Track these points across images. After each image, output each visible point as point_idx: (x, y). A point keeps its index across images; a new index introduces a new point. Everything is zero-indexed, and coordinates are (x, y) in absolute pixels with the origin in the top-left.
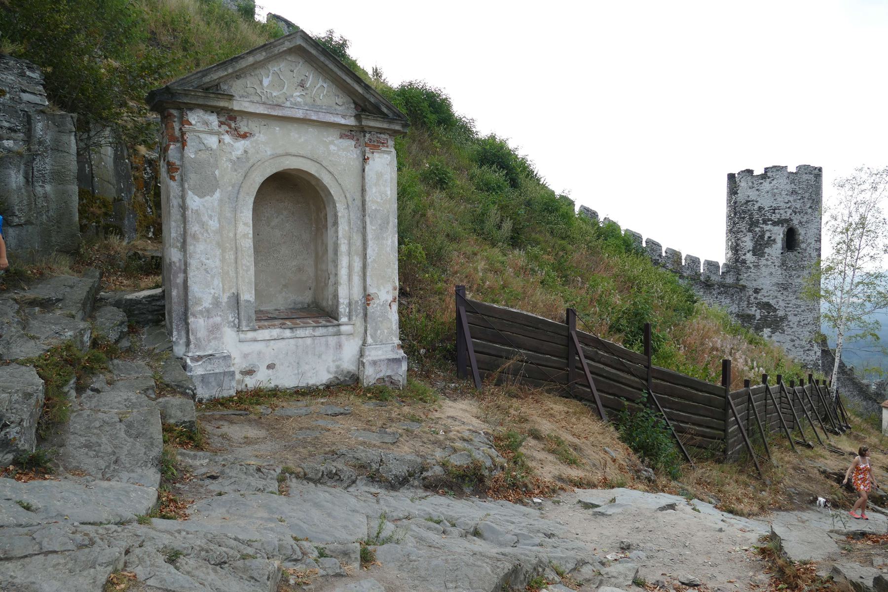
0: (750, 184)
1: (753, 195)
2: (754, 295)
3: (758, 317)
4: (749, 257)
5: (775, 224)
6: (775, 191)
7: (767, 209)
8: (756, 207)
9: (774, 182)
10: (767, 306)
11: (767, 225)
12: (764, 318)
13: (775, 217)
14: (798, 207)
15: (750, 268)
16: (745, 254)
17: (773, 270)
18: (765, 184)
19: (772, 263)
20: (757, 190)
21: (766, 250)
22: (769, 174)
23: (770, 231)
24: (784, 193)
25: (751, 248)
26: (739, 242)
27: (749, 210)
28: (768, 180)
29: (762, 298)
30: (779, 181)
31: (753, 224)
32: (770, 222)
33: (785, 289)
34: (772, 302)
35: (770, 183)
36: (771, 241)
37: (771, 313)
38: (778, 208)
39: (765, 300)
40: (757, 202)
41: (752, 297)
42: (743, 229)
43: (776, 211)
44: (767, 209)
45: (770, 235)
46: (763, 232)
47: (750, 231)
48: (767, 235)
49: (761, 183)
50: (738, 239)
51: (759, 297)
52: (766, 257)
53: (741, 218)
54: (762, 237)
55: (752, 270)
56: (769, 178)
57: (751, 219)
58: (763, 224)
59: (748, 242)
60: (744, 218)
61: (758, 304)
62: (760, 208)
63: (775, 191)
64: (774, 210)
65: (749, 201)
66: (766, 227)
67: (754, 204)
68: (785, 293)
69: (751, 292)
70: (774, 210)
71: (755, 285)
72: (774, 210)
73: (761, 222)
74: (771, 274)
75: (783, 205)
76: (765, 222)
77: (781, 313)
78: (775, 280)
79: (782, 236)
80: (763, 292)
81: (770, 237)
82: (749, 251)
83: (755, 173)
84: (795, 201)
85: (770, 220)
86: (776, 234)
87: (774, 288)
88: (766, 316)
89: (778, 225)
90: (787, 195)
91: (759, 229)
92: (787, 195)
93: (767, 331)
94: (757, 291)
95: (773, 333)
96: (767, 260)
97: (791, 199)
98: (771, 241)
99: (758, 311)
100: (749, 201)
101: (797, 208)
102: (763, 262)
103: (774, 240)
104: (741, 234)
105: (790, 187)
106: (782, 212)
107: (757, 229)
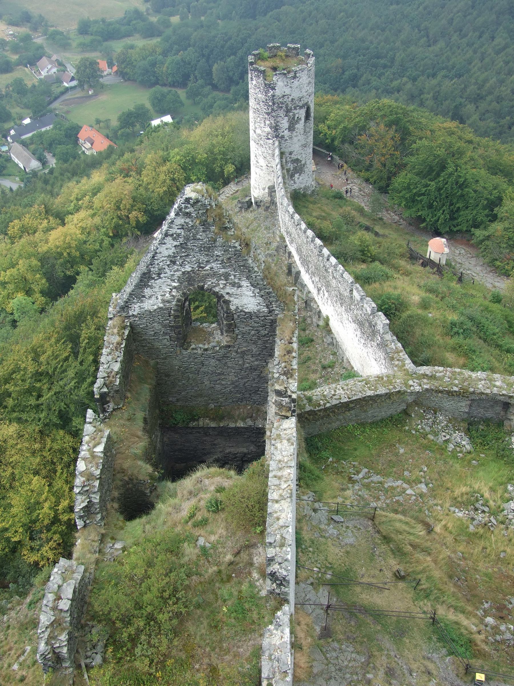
0: (286, 83)
1: (287, 91)
3: (292, 168)
4: (286, 133)
7: (296, 99)
8: (290, 99)
10: (297, 161)
11: (296, 109)
12: (295, 168)
13: (301, 104)
15: (287, 140)
16: (283, 132)
18: (295, 82)
21: (297, 126)
22: (297, 75)
24: (305, 85)
26: (278, 124)
31: (288, 111)
33: (305, 147)
34: (299, 157)
36: (299, 119)
38: (302, 97)
39: (296, 157)
42: (282, 115)
44: (296, 99)
46: (294, 115)
47: (286, 116)
48: (297, 116)
54: (294, 118)
57: (287, 107)
59: (285, 123)
60: (282, 107)
62: (292, 99)
69: (287, 155)
70: (300, 99)
71: (290, 150)
75: (305, 94)
77: (303, 162)
80: (295, 153)
85: (298, 106)
87: (301, 148)
88: (296, 167)
94: (291, 153)
95: (300, 175)
97: (308, 88)
98: (299, 119)
106: (304, 99)
107: (291, 114)
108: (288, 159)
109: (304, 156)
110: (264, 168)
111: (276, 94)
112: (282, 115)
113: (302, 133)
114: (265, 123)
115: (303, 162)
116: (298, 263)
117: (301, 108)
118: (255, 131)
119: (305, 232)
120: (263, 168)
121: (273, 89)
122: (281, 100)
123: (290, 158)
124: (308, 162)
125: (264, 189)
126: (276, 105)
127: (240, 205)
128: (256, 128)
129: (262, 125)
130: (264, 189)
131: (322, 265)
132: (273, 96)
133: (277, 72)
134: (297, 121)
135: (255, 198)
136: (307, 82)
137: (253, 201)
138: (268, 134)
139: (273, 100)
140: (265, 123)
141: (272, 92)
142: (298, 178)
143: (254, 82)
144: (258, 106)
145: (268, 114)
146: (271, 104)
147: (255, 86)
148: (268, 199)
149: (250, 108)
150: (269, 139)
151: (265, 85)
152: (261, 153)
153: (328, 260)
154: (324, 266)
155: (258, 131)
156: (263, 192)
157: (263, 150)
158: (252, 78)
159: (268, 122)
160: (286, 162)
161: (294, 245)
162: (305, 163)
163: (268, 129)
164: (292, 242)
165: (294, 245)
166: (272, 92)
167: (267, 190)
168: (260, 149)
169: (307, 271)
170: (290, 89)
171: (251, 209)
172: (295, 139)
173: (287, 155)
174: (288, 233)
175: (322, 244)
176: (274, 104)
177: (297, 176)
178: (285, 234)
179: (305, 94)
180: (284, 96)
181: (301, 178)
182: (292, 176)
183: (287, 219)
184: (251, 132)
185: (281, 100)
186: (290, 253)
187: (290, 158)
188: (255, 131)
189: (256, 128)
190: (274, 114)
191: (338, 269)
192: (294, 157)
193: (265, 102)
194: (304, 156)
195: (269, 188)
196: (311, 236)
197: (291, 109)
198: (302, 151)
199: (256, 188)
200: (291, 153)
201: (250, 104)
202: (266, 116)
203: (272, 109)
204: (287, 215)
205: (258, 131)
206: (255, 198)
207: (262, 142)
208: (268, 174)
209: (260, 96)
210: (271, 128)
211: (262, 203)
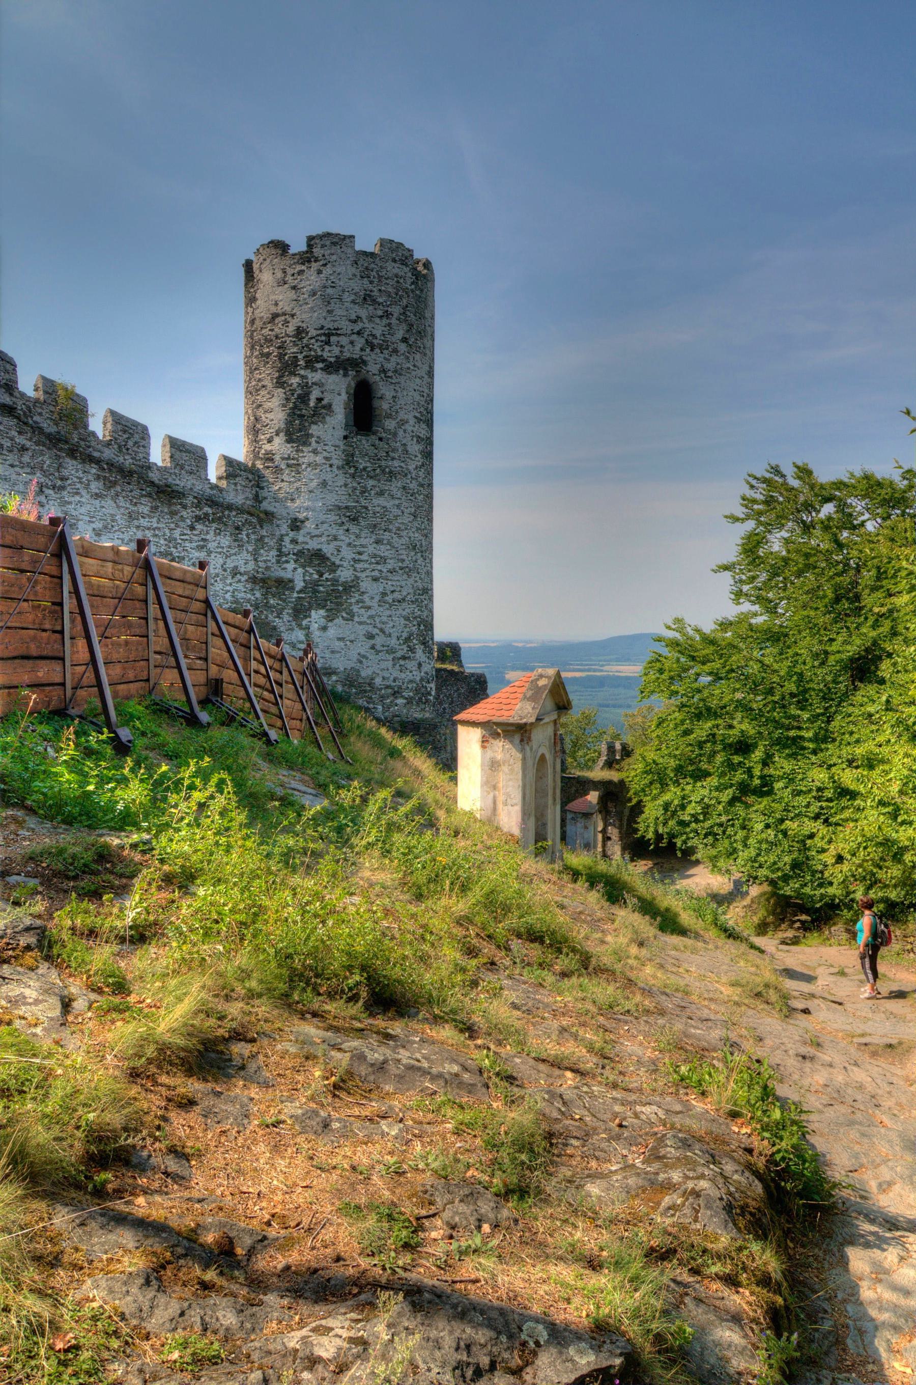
0: (279, 275)
2: (292, 534)
3: (299, 585)
5: (331, 368)
7: (313, 333)
8: (291, 329)
9: (328, 270)
11: (314, 370)
12: (312, 587)
13: (330, 353)
14: (378, 333)
19: (326, 458)
20: (294, 288)
21: (314, 430)
22: (317, 251)
24: (347, 297)
26: (260, 412)
27: (277, 337)
28: (315, 266)
29: (307, 539)
30: (339, 270)
32: (320, 365)
33: (354, 520)
35: (319, 272)
37: (326, 576)
38: (336, 332)
39: (313, 545)
40: (293, 316)
41: (287, 539)
43: (333, 339)
45: (320, 395)
48: (315, 394)
49: (301, 272)
51: (301, 539)
52: (314, 444)
54: (304, 398)
57: (281, 356)
60: (268, 355)
61: (299, 554)
64: (328, 335)
66: (314, 377)
67: (286, 322)
68: (354, 529)
69: (284, 528)
70: (328, 335)
72: (328, 335)
73: (302, 363)
76: (310, 363)
77: (345, 574)
79: (344, 396)
80: (309, 526)
81: (320, 400)
83: (292, 251)
84: (371, 318)
86: (332, 391)
87: (332, 517)
88: (316, 583)
89: (337, 371)
90: (353, 302)
92: (353, 302)
93: (317, 616)
95: (329, 618)
96: (315, 452)
97: (363, 313)
99: (300, 570)
101: (374, 336)
103: (329, 407)
104: (263, 392)
105: (358, 285)
106: (344, 340)
107: (295, 381)
108: (288, 546)
112: (267, 382)
113: (335, 462)
123: (294, 541)
142: (324, 629)
170: (292, 295)
180: (275, 316)
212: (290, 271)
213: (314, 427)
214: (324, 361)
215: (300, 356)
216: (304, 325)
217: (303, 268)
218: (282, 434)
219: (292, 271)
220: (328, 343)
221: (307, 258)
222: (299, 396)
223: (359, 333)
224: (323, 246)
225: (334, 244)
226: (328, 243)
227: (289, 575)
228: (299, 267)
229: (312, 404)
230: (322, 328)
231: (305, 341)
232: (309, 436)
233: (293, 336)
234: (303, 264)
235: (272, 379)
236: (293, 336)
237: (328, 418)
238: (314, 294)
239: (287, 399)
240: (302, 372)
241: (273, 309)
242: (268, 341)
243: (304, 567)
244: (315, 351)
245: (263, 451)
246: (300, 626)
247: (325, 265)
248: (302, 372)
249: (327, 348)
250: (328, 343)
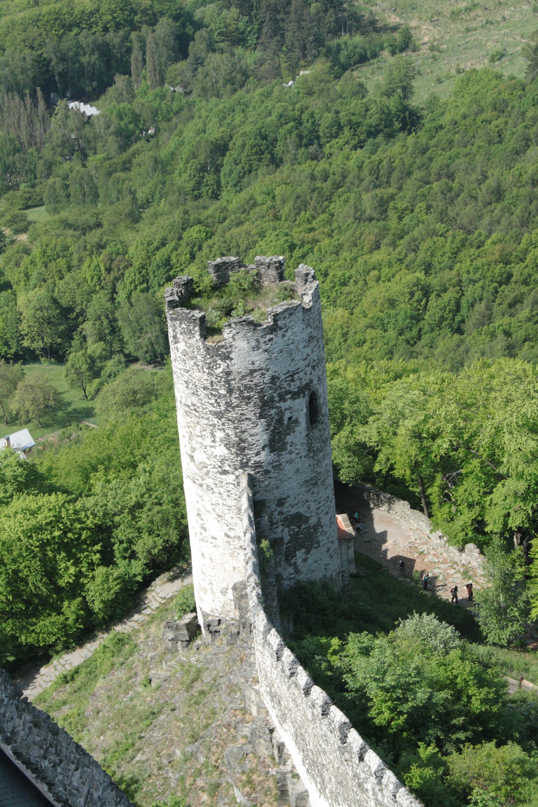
0: (254, 344)
2: (279, 509)
3: (287, 538)
6: (292, 346)
7: (283, 377)
9: (289, 334)
10: (299, 518)
11: (285, 400)
12: (295, 537)
13: (294, 387)
17: (299, 465)
19: (298, 454)
20: (266, 351)
21: (289, 439)
22: (280, 323)
23: (290, 408)
24: (301, 346)
25: (267, 443)
26: (245, 436)
27: (256, 385)
28: (280, 333)
29: (290, 509)
32: (289, 396)
33: (315, 484)
34: (302, 510)
35: (284, 336)
36: (293, 422)
37: (304, 526)
39: (293, 511)
41: (276, 513)
43: (296, 377)
44: (283, 377)
46: (281, 414)
47: (261, 416)
48: (287, 415)
50: (243, 432)
51: (285, 510)
52: (289, 448)
53: (244, 398)
54: (280, 421)
55: (272, 475)
56: (281, 329)
57: (261, 398)
58: (279, 401)
60: (249, 398)
61: (286, 519)
63: (292, 346)
64: (292, 376)
65: (255, 371)
66: (284, 405)
68: (315, 490)
69: (273, 507)
70: (292, 376)
71: (277, 494)
72: (292, 376)
73: (277, 399)
74: (298, 471)
75: (301, 364)
76: (282, 398)
77: (313, 521)
78: (302, 478)
79: (305, 410)
80: (291, 501)
81: (290, 419)
82: (263, 449)
84: (312, 352)
85: (288, 392)
87: (304, 489)
88: (298, 534)
89: (299, 397)
91: (275, 410)
92: (304, 347)
94: (281, 503)
95: (308, 552)
97: (308, 350)
98: (293, 422)
99: (286, 530)
100: (255, 371)
101: (314, 361)
102: (285, 456)
103: (297, 421)
104: (247, 422)
106: (302, 375)
107: (273, 412)
108: (276, 517)
109: (313, 507)
110: (221, 540)
111: (234, 368)
112: (251, 415)
113: (303, 454)
114: (213, 435)
115: (313, 521)
116: (301, 770)
117: (295, 395)
118: (192, 457)
119: (307, 692)
120: (218, 542)
121: (226, 357)
122: (245, 382)
123: (280, 513)
124: (325, 520)
125: (224, 592)
126: (236, 394)
127: (170, 635)
128: (193, 449)
129: (208, 441)
130: (224, 592)
131: (350, 773)
132: (228, 374)
133: (232, 320)
134: (288, 427)
135: (205, 615)
136: (305, 336)
137: (201, 621)
138: (222, 461)
139: (228, 382)
140: (213, 435)
141: (223, 366)
142: (305, 560)
143: (181, 346)
144: (194, 399)
145: (219, 415)
146: (223, 392)
147: (185, 353)
148: (235, 614)
149: (178, 404)
150: (225, 472)
151: (208, 349)
152: (209, 507)
153: (361, 759)
154: (356, 775)
155: (200, 456)
156: (222, 599)
157: (215, 498)
158: (175, 337)
159: (220, 435)
160: (272, 523)
161: (288, 726)
162: (319, 524)
163: (221, 451)
164: (283, 718)
165: (288, 726)
166: (223, 366)
167: (230, 594)
168: (206, 498)
169: (322, 791)
171: (198, 642)
172: (288, 469)
173: (273, 507)
174: (273, 696)
175: (345, 719)
176: (230, 391)
177: (300, 554)
178: (267, 700)
179: (301, 364)
180: (252, 372)
181: (310, 560)
182: (290, 555)
183: (268, 662)
184: (185, 459)
185: (245, 382)
186: (281, 747)
187: (280, 513)
188: (192, 457)
189: (193, 449)
190: (232, 415)
191: (384, 781)
192: (289, 510)
193: (210, 389)
194: (313, 507)
195: (235, 588)
196: (320, 702)
197: (272, 399)
198: (309, 496)
199: (205, 592)
200: (281, 503)
201: (177, 395)
202: (216, 421)
203: (228, 404)
204: (267, 654)
205: (200, 456)
206: (205, 615)
207: (209, 481)
208: (232, 555)
209: (197, 375)
210: (228, 446)
211: (223, 626)
212: (262, 340)
213: (288, 437)
214: (290, 392)
215: (275, 395)
216: (276, 374)
217: (272, 336)
218: (266, 449)
219: (264, 340)
220: (293, 380)
221: (273, 329)
222: (277, 420)
223: (308, 365)
224: (284, 318)
225: (291, 314)
226: (287, 315)
227: (279, 535)
228: (269, 337)
229: (286, 422)
230: (289, 372)
231: (278, 384)
232: (285, 444)
233: (270, 383)
234: (271, 333)
235: (255, 414)
236: (270, 383)
237: (296, 429)
238: (281, 351)
239: (269, 425)
240: (278, 405)
241: (251, 367)
242: (248, 388)
243: (288, 526)
244: (285, 388)
245: (252, 462)
246: (290, 565)
247: (286, 331)
248: (278, 405)
249: (292, 384)
250: (293, 380)
